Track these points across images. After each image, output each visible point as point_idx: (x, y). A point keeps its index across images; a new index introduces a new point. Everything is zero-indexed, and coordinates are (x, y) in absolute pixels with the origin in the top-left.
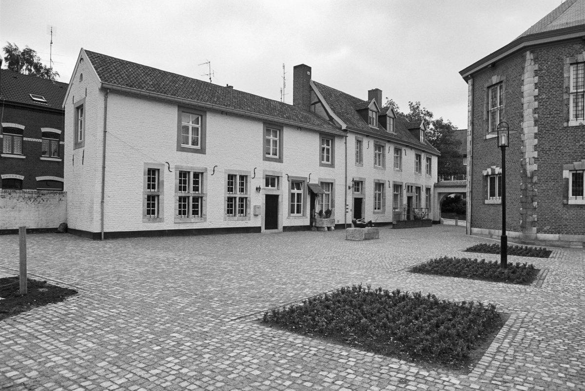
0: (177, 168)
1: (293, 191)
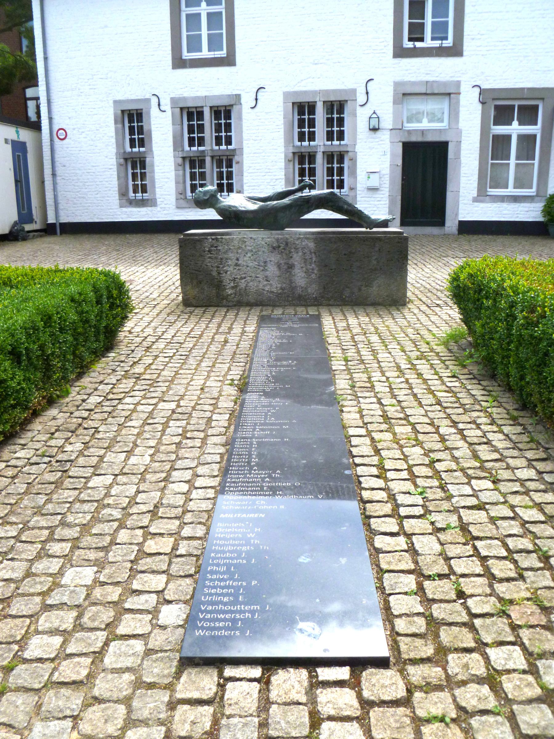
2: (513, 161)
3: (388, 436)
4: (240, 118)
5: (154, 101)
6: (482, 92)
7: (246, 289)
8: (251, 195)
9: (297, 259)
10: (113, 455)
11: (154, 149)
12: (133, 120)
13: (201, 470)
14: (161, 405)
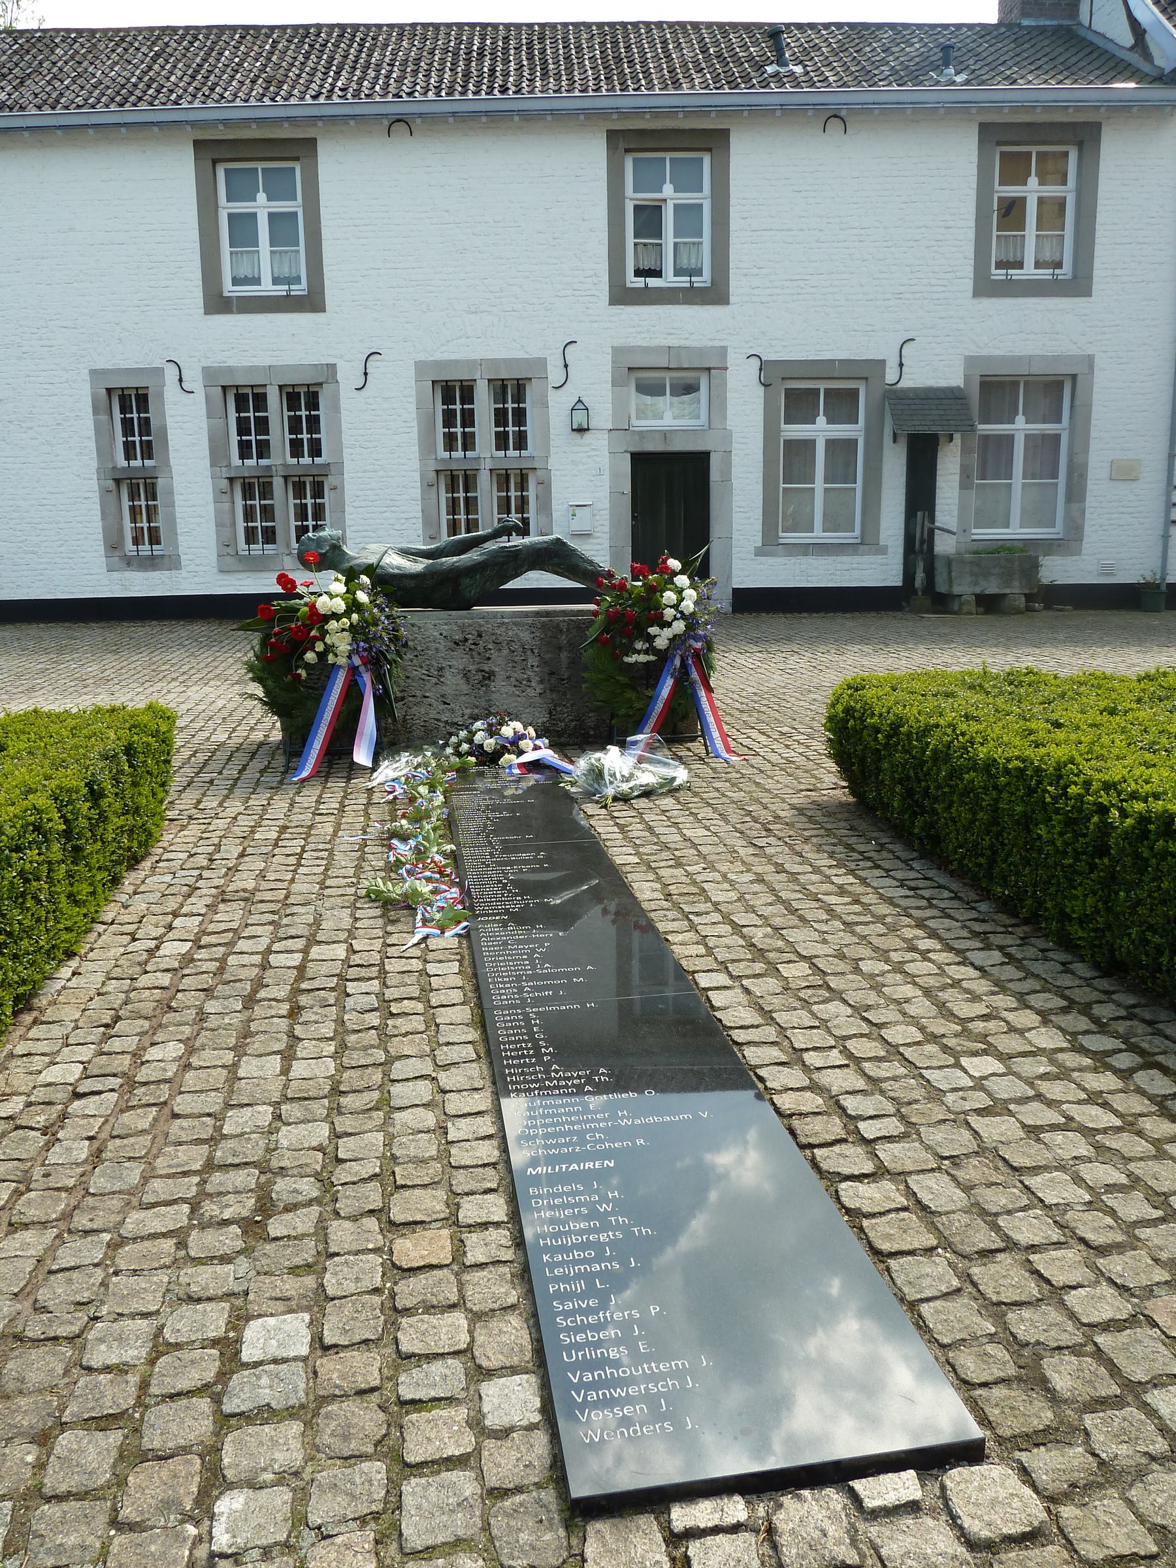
0: (208, 373)
1: (797, 431)
2: (819, 485)
3: (772, 984)
4: (336, 408)
5: (171, 373)
6: (764, 366)
7: (405, 720)
8: (405, 545)
9: (498, 663)
10: (255, 1062)
11: (172, 461)
12: (131, 408)
13: (444, 1079)
14: (315, 952)
